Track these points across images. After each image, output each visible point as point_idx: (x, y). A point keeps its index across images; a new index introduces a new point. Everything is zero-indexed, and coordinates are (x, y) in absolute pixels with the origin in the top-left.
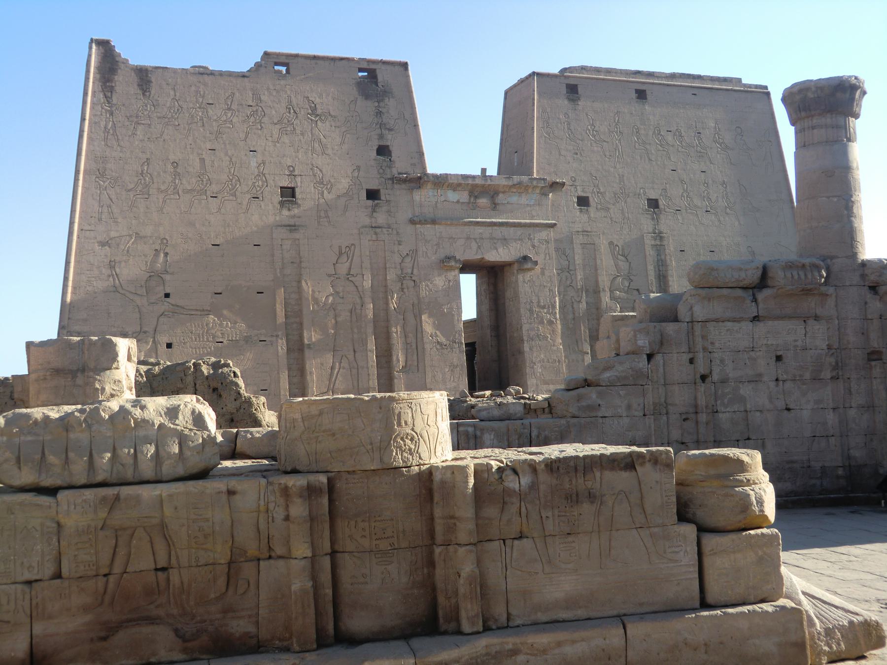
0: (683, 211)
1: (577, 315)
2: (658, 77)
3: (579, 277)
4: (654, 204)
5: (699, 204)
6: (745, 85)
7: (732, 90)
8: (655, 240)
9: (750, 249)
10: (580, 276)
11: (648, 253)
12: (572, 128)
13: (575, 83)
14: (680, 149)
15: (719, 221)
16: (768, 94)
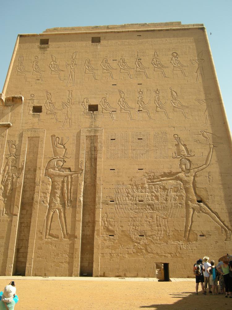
0: (118, 111)
1: (14, 187)
2: (111, 28)
3: (21, 160)
4: (93, 108)
5: (133, 106)
6: (183, 26)
7: (171, 30)
8: (90, 131)
9: (177, 136)
10: (24, 159)
11: (81, 141)
12: (39, 64)
13: (48, 38)
14: (122, 71)
15: (150, 117)
16: (203, 29)
